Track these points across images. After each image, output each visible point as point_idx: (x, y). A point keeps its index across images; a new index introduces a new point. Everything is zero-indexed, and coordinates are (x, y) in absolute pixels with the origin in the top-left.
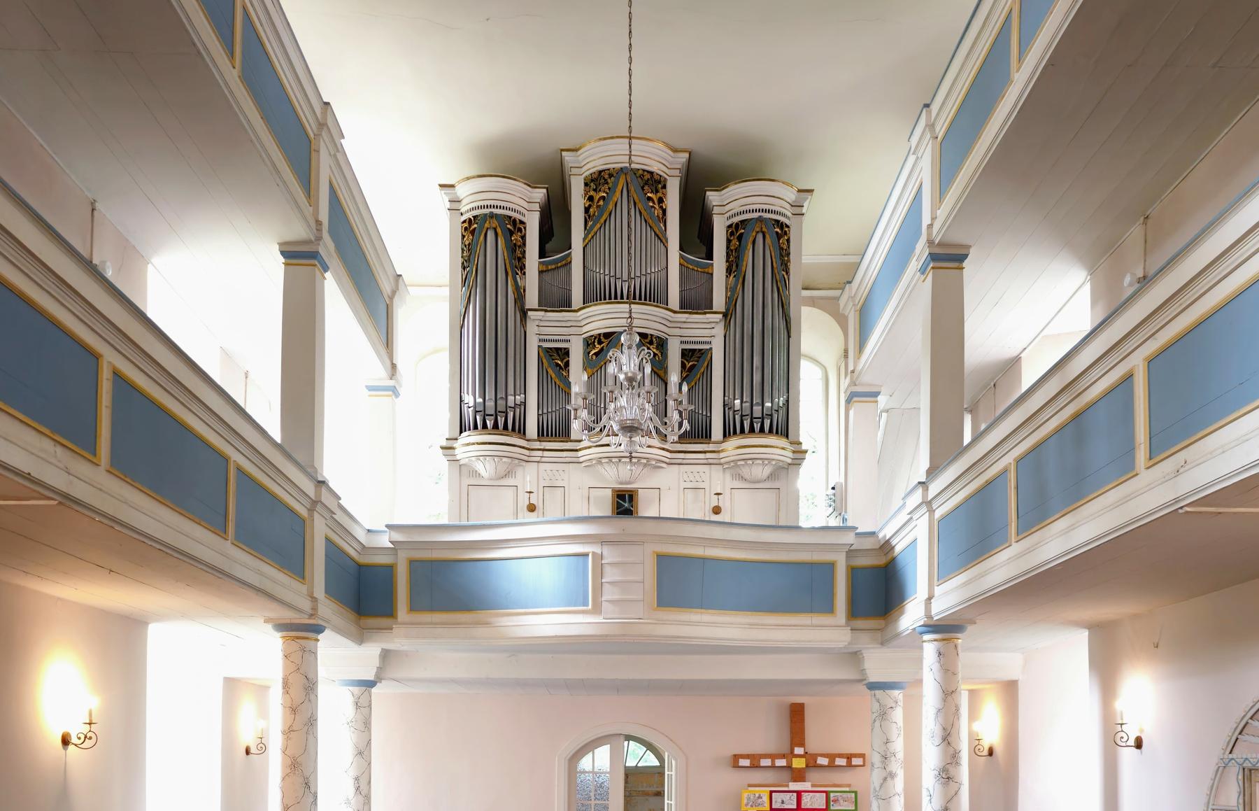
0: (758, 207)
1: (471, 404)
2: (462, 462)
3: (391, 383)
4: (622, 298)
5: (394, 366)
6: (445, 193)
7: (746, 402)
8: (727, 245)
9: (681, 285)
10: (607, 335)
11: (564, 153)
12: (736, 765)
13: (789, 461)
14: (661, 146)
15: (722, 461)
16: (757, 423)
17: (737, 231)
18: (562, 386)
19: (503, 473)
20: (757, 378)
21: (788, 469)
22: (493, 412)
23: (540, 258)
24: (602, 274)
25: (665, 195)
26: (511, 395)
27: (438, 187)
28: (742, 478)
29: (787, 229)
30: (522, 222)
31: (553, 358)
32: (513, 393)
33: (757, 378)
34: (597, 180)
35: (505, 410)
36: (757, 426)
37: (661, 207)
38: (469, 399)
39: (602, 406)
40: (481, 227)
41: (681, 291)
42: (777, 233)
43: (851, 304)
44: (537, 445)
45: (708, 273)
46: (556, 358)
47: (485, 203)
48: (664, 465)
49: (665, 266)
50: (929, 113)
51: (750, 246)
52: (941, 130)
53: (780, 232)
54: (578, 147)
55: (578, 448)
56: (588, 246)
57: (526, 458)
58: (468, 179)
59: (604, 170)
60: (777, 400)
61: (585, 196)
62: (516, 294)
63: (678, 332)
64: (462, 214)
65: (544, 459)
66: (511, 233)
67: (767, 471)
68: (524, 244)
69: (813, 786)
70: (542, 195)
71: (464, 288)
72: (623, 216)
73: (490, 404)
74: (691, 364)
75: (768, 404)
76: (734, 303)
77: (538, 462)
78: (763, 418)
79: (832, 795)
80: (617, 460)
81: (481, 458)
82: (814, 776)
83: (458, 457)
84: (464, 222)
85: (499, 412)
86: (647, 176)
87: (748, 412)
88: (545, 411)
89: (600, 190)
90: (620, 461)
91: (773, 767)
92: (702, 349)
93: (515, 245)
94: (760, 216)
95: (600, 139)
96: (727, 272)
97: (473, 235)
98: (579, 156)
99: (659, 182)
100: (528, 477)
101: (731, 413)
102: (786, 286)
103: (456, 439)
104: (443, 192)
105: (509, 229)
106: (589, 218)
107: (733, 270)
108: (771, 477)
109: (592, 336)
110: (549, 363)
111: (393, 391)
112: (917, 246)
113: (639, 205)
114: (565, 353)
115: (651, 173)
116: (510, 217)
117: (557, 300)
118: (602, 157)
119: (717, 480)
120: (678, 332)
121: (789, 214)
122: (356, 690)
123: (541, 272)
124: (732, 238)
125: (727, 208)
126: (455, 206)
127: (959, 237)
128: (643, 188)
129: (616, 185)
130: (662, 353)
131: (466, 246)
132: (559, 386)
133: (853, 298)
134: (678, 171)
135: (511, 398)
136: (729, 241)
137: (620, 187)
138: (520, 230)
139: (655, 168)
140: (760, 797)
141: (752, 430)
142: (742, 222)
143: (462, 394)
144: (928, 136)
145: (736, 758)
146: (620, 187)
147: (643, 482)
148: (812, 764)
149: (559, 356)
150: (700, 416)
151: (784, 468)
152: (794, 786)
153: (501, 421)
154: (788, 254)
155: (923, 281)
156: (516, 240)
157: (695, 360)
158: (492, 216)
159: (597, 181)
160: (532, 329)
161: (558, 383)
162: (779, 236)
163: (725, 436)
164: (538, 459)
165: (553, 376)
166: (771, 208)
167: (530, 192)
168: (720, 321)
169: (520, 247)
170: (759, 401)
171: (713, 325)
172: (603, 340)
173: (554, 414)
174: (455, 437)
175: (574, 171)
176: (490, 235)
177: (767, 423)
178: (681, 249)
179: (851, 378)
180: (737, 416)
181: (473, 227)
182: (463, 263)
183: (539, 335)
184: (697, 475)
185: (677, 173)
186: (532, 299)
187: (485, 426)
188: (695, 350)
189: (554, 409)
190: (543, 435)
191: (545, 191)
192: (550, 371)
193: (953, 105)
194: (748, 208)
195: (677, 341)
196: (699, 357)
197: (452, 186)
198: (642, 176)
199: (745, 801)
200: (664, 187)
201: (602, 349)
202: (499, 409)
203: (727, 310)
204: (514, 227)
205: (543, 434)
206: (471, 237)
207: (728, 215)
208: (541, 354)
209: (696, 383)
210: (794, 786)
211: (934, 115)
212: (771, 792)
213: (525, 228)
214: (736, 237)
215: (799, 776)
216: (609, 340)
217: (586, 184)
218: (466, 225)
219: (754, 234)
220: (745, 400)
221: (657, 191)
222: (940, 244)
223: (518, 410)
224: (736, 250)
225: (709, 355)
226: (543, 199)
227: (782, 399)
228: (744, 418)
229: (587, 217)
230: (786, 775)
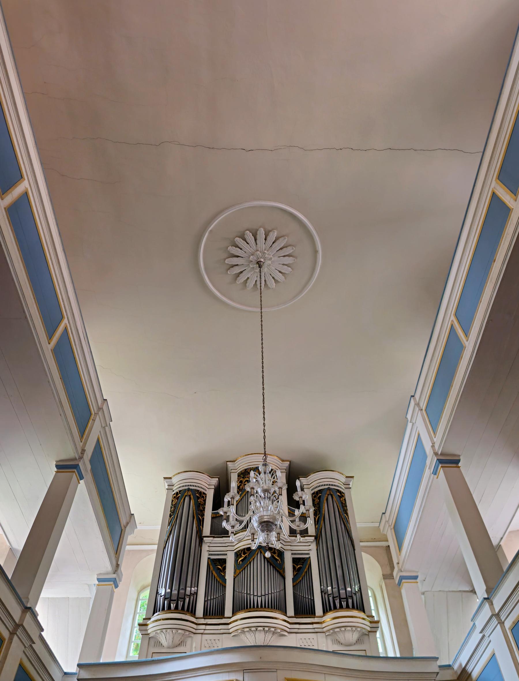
0: (327, 483)
1: (163, 594)
2: (151, 635)
3: (114, 576)
5: (118, 566)
6: (166, 482)
7: (335, 588)
8: (313, 502)
11: (228, 463)
13: (369, 629)
14: (276, 458)
15: (325, 629)
16: (344, 602)
18: (221, 581)
19: (177, 642)
20: (339, 572)
21: (368, 635)
22: (176, 598)
23: (212, 511)
26: (189, 587)
27: (163, 478)
29: (343, 494)
30: (204, 493)
31: (216, 565)
32: (190, 586)
33: (339, 572)
34: (244, 473)
35: (183, 597)
36: (344, 604)
38: (162, 591)
39: (245, 592)
40: (183, 495)
42: (338, 495)
43: (388, 526)
44: (203, 621)
45: (304, 517)
47: (186, 484)
48: (286, 634)
50: (415, 399)
51: (325, 501)
52: (423, 405)
53: (340, 495)
54: (235, 460)
55: (229, 622)
56: (239, 505)
57: (194, 631)
58: (179, 473)
59: (248, 469)
60: (354, 586)
61: (238, 481)
62: (198, 528)
63: (289, 548)
64: (173, 491)
65: (206, 632)
66: (198, 498)
67: (355, 636)
68: (205, 504)
70: (216, 481)
71: (169, 527)
73: (175, 592)
74: (299, 566)
75: (349, 589)
76: (320, 531)
77: (202, 634)
78: (347, 599)
80: (254, 629)
81: (164, 630)
83: (149, 632)
84: (174, 494)
85: (180, 598)
88: (209, 598)
89: (246, 477)
90: (257, 629)
92: (305, 558)
93: (200, 504)
94: (329, 487)
95: (246, 455)
96: (314, 515)
97: (178, 500)
98: (235, 464)
101: (326, 596)
102: (348, 522)
103: (150, 619)
104: (165, 481)
105: (197, 496)
106: (240, 491)
107: (318, 514)
108: (359, 641)
109: (240, 550)
110: (214, 568)
111: (114, 582)
112: (427, 462)
116: (198, 491)
118: (247, 463)
120: (289, 548)
121: (343, 488)
123: (213, 518)
124: (315, 499)
126: (171, 487)
127: (453, 449)
130: (281, 560)
131: (173, 505)
132: (219, 582)
133: (387, 521)
134: (285, 470)
135: (188, 589)
138: (203, 497)
141: (341, 607)
142: (320, 490)
143: (158, 588)
144: (417, 409)
149: (220, 563)
150: (307, 599)
151: (366, 634)
153: (180, 604)
154: (346, 506)
155: (437, 478)
156: (200, 501)
158: (189, 490)
160: (205, 548)
161: (218, 579)
164: (202, 631)
165: (216, 575)
166: (334, 484)
167: (210, 480)
168: (313, 541)
169: (202, 505)
170: (343, 587)
171: (309, 544)
172: (246, 552)
173: (215, 600)
174: (149, 617)
175: (233, 471)
176: (187, 499)
177: (350, 601)
178: (288, 505)
179: (398, 567)
180: (330, 598)
181: (178, 496)
182: (170, 514)
183: (209, 551)
184: (308, 641)
185: (284, 471)
186: (207, 530)
187: (169, 608)
188: (301, 558)
189: (215, 597)
190: (207, 615)
191: (217, 479)
192: (214, 573)
193: (424, 403)
195: (290, 552)
196: (303, 563)
197: (170, 478)
201: (246, 557)
202: (180, 596)
203: (317, 534)
205: (207, 614)
206: (177, 501)
207: (312, 488)
208: (210, 563)
209: (302, 578)
211: (417, 399)
213: (206, 497)
214: (317, 498)
216: (250, 551)
217: (238, 476)
219: (327, 495)
220: (334, 587)
222: (442, 454)
223: (192, 597)
224: (318, 504)
225: (309, 561)
226: (217, 484)
227: (356, 586)
228: (335, 599)
229: (239, 490)
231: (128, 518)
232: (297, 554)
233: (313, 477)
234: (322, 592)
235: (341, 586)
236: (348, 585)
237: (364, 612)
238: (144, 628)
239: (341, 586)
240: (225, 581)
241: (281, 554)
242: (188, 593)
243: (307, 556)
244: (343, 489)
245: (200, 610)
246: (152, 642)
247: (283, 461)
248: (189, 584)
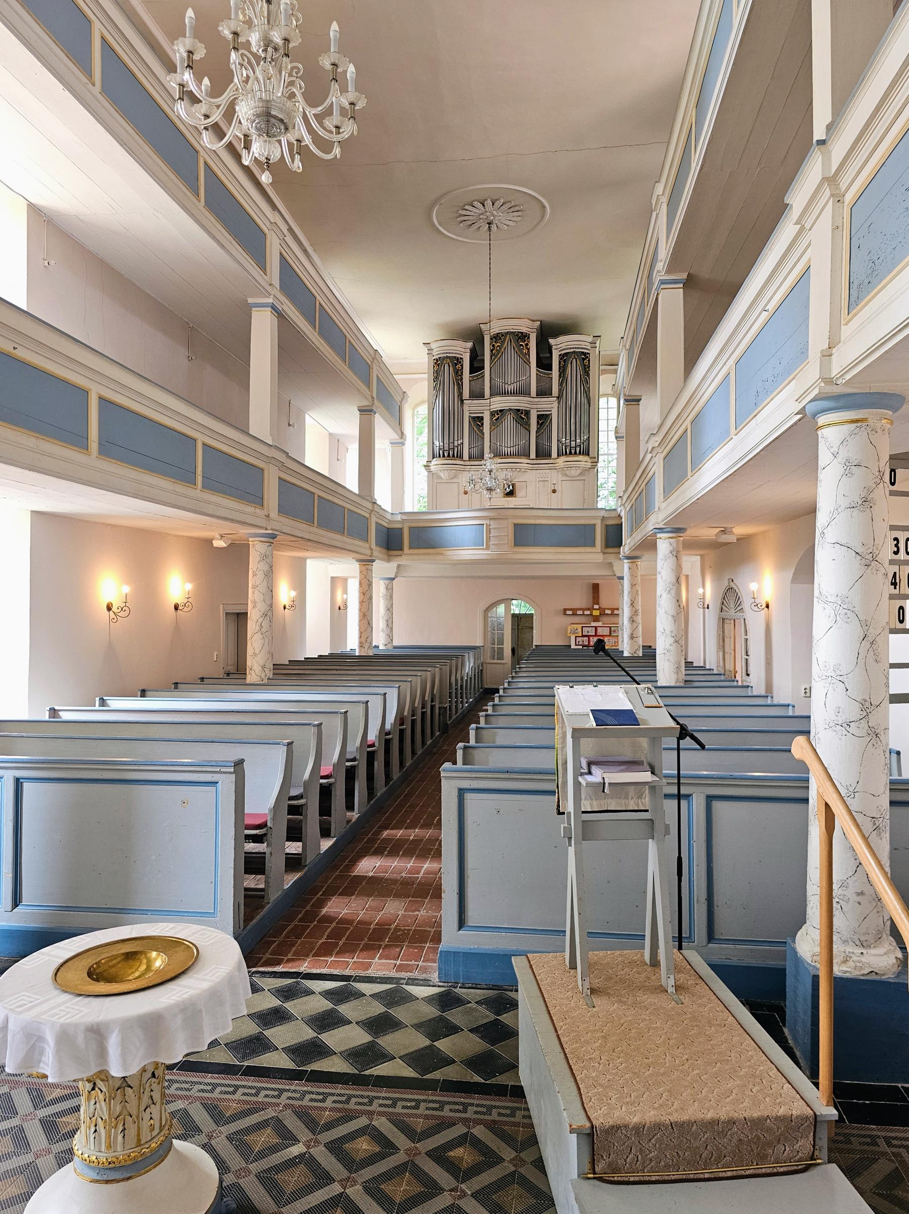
0: (573, 346)
1: (438, 445)
4: (508, 394)
9: (537, 384)
10: (501, 411)
12: (565, 614)
17: (564, 358)
23: (470, 373)
24: (498, 381)
25: (529, 342)
28: (567, 475)
30: (461, 358)
36: (573, 451)
37: (527, 348)
38: (437, 443)
41: (537, 387)
44: (468, 463)
46: (477, 421)
49: (528, 375)
51: (570, 365)
63: (535, 406)
66: (456, 364)
67: (579, 472)
68: (462, 368)
69: (603, 624)
72: (510, 353)
73: (446, 446)
75: (578, 441)
78: (576, 447)
79: (612, 628)
82: (605, 619)
86: (520, 335)
87: (569, 444)
91: (583, 614)
99: (526, 336)
100: (464, 478)
108: (581, 474)
113: (516, 349)
114: (482, 418)
115: (522, 333)
117: (477, 395)
119: (554, 477)
120: (535, 406)
122: (387, 582)
125: (559, 346)
128: (518, 341)
129: (505, 340)
136: (560, 362)
137: (507, 341)
138: (460, 362)
139: (524, 330)
140: (577, 629)
142: (566, 353)
145: (565, 610)
146: (507, 341)
147: (518, 479)
148: (603, 614)
152: (593, 624)
154: (589, 367)
157: (544, 419)
158: (447, 357)
159: (496, 338)
160: (466, 408)
162: (584, 359)
163: (558, 456)
176: (446, 366)
177: (578, 449)
187: (444, 456)
192: (475, 428)
194: (567, 347)
197: (429, 343)
198: (517, 335)
199: (569, 632)
200: (529, 338)
201: (498, 418)
203: (559, 395)
204: (456, 362)
210: (593, 624)
212: (582, 627)
215: (596, 619)
217: (491, 339)
218: (435, 361)
221: (525, 341)
230: (591, 618)
231: (401, 395)
232: (541, 411)
233: (562, 339)
234: (558, 441)
235: (573, 438)
236: (577, 438)
237: (589, 455)
238: (428, 468)
239: (573, 438)
240: (483, 434)
241: (527, 413)
242: (456, 444)
243: (549, 413)
244: (589, 350)
245: (466, 456)
246: (434, 475)
247: (534, 321)
248: (456, 438)
